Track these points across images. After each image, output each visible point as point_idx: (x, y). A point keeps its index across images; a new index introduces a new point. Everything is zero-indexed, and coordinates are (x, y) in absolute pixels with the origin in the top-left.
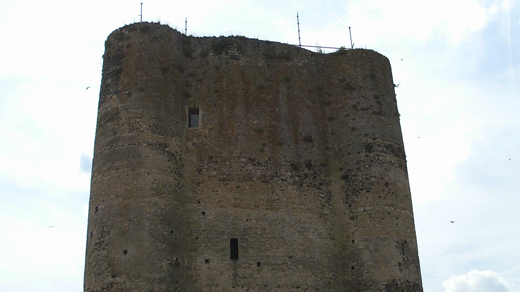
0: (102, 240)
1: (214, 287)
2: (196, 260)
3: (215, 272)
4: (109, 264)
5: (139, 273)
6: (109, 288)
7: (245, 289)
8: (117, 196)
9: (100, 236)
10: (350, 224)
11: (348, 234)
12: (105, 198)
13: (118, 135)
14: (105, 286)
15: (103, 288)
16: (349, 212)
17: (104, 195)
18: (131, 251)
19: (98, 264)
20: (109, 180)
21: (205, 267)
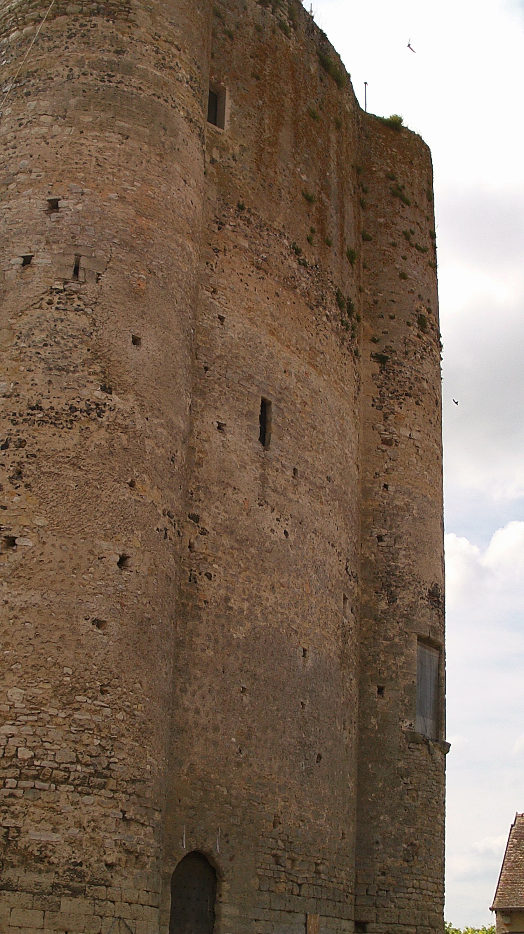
0: (74, 286)
1: (230, 491)
2: (202, 416)
3: (233, 457)
4: (96, 355)
5: (160, 402)
6: (94, 415)
7: (275, 515)
8: (122, 199)
9: (69, 274)
10: (383, 451)
11: (377, 470)
12: (85, 190)
13: (127, 58)
14: (82, 405)
15: (73, 409)
16: (382, 428)
17: (85, 179)
18: (149, 343)
19: (58, 343)
20: (100, 151)
21: (217, 438)
